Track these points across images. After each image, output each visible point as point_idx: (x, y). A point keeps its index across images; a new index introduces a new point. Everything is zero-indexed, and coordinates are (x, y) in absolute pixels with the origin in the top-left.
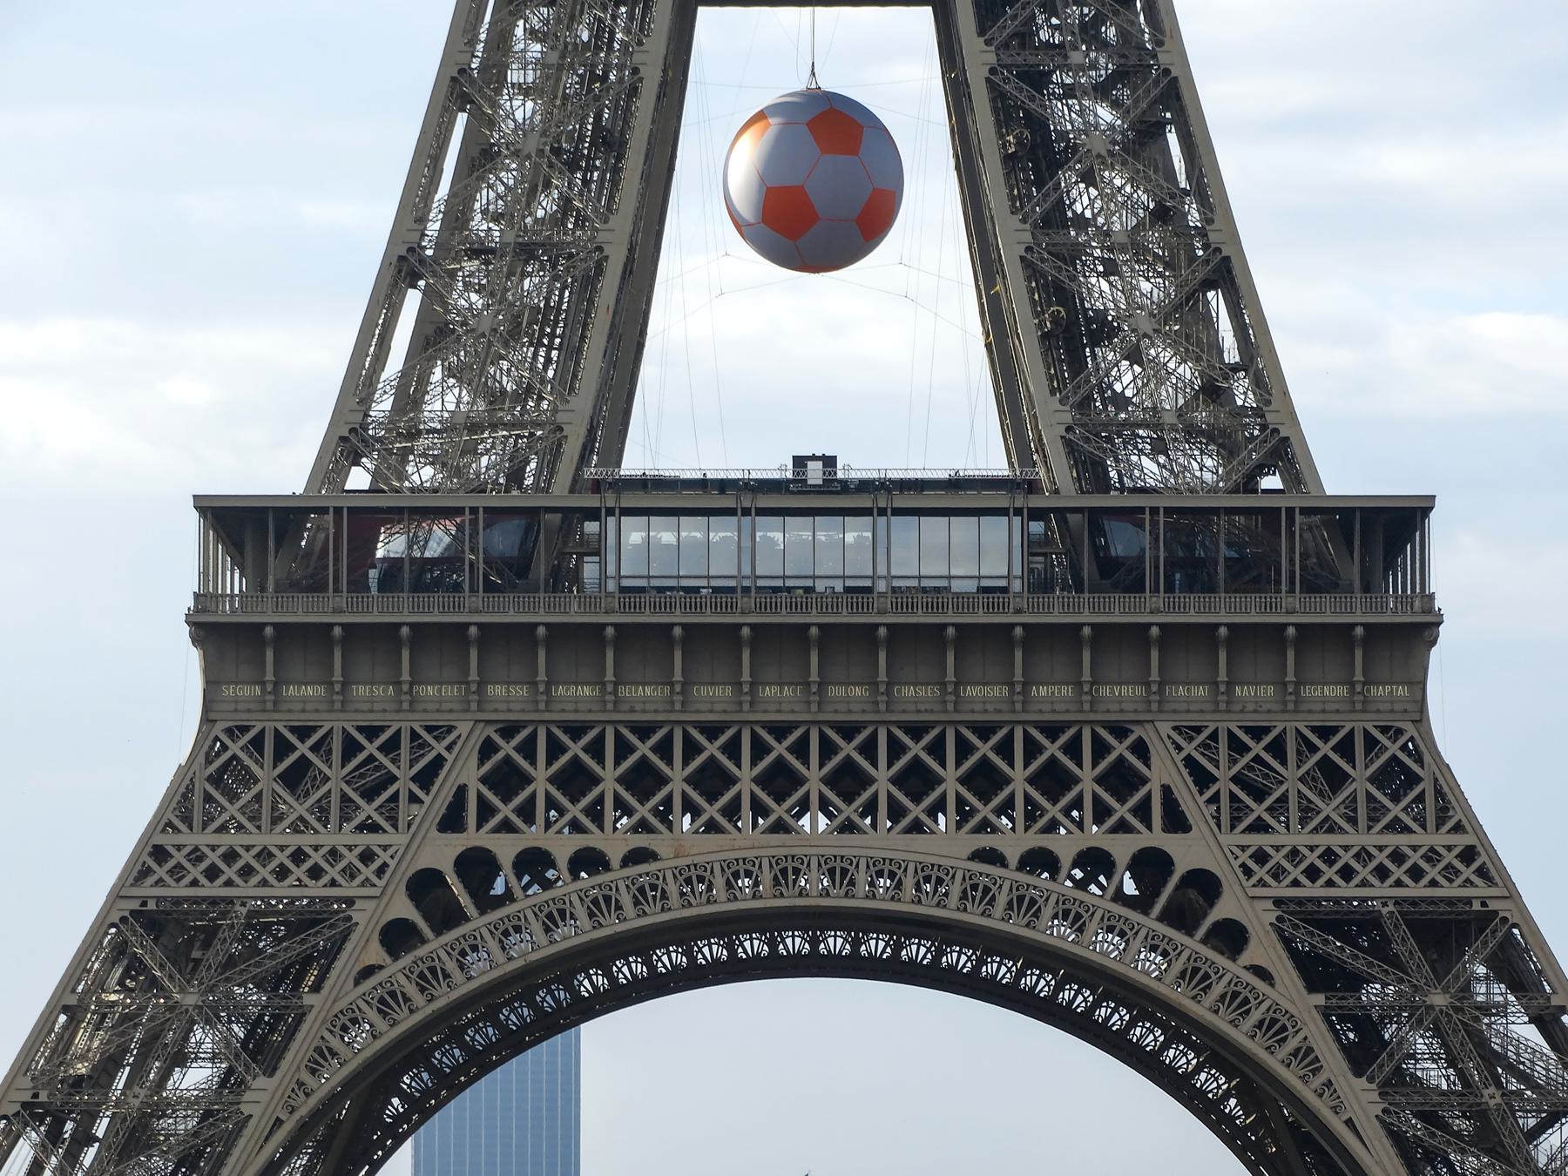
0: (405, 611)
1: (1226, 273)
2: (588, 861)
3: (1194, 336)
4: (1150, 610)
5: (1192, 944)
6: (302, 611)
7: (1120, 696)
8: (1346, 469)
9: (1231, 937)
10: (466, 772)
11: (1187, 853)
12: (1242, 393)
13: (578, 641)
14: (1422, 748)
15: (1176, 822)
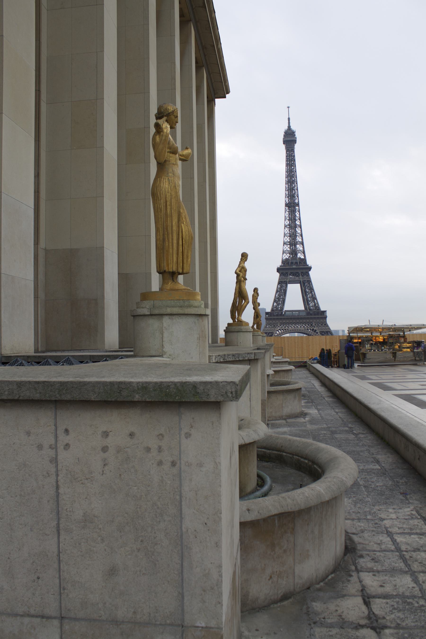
0: (276, 317)
1: (316, 299)
2: (285, 330)
3: (314, 302)
4: (313, 316)
5: (315, 333)
6: (271, 317)
7: (311, 321)
8: (322, 309)
9: (317, 333)
10: (279, 325)
11: (315, 329)
12: (317, 305)
13: (284, 319)
14: (326, 323)
15: (314, 327)
